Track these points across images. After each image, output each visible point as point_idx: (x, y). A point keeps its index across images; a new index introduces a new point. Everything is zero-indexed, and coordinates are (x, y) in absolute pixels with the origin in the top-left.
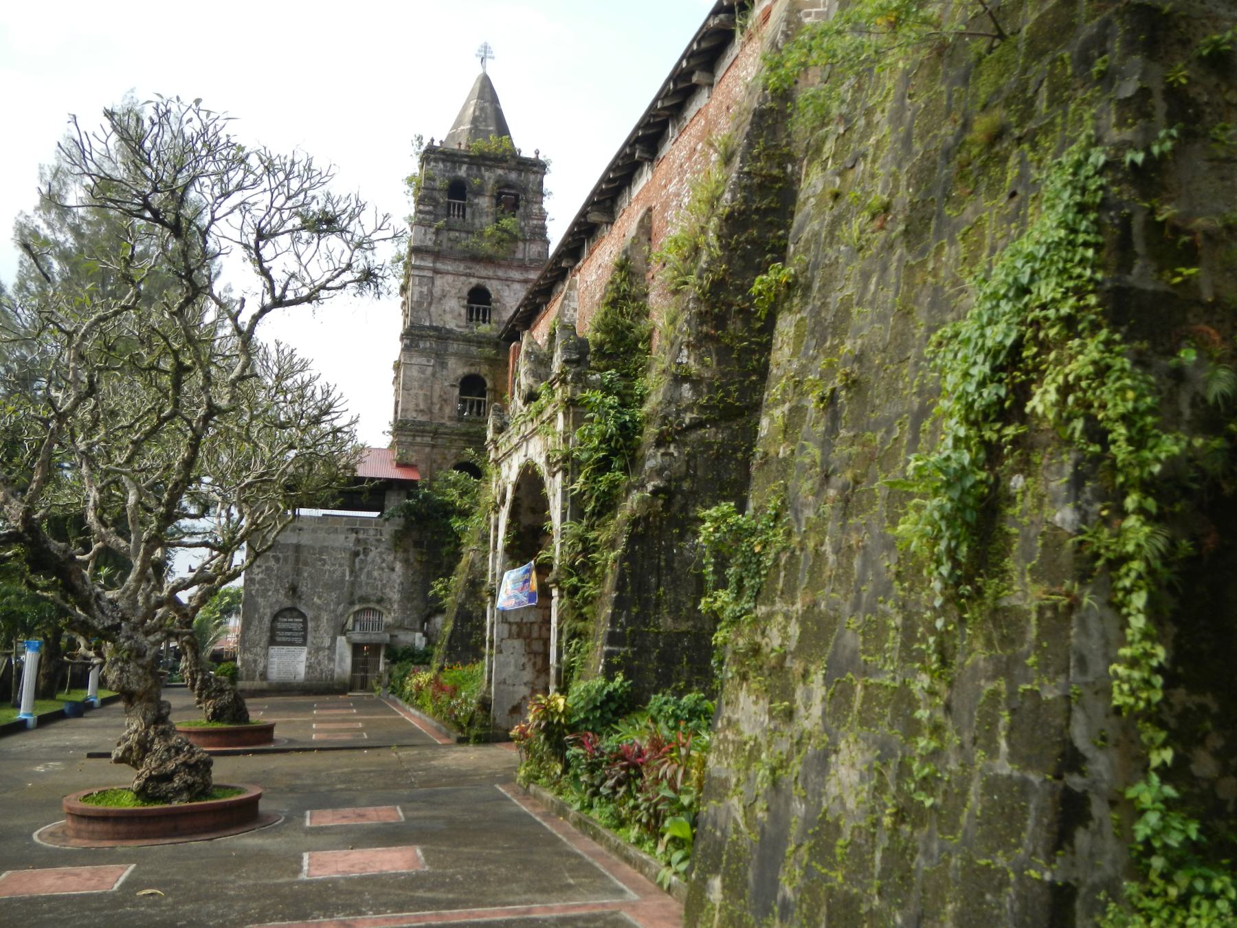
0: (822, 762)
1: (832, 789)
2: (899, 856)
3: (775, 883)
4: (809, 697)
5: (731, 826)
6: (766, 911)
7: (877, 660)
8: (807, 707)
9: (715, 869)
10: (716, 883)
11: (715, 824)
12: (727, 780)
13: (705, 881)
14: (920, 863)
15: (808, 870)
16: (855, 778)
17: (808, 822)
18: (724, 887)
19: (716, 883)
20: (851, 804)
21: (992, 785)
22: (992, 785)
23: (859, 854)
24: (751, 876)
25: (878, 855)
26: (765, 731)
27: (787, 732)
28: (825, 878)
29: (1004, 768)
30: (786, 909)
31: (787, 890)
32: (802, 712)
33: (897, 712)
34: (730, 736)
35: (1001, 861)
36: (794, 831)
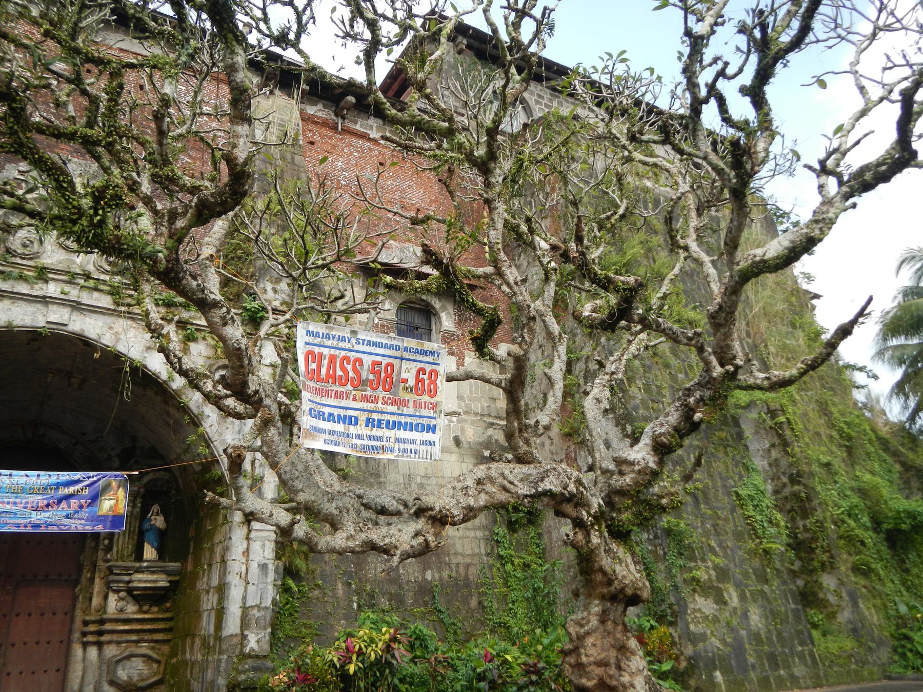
0: (745, 615)
1: (752, 623)
2: (779, 635)
3: (746, 661)
4: (730, 594)
5: (715, 650)
6: (746, 671)
7: (749, 582)
8: (731, 599)
9: (715, 669)
10: (718, 674)
11: (706, 652)
12: (705, 633)
13: (712, 676)
14: (785, 634)
15: (755, 651)
16: (758, 618)
17: (749, 636)
18: (722, 674)
19: (718, 674)
20: (760, 625)
21: (793, 611)
22: (793, 611)
23: (769, 639)
24: (733, 663)
25: (774, 638)
26: (716, 610)
27: (727, 608)
28: (762, 651)
29: (793, 606)
30: (753, 666)
31: (751, 660)
32: (729, 601)
33: (762, 597)
34: (698, 615)
35: (800, 627)
36: (746, 640)
